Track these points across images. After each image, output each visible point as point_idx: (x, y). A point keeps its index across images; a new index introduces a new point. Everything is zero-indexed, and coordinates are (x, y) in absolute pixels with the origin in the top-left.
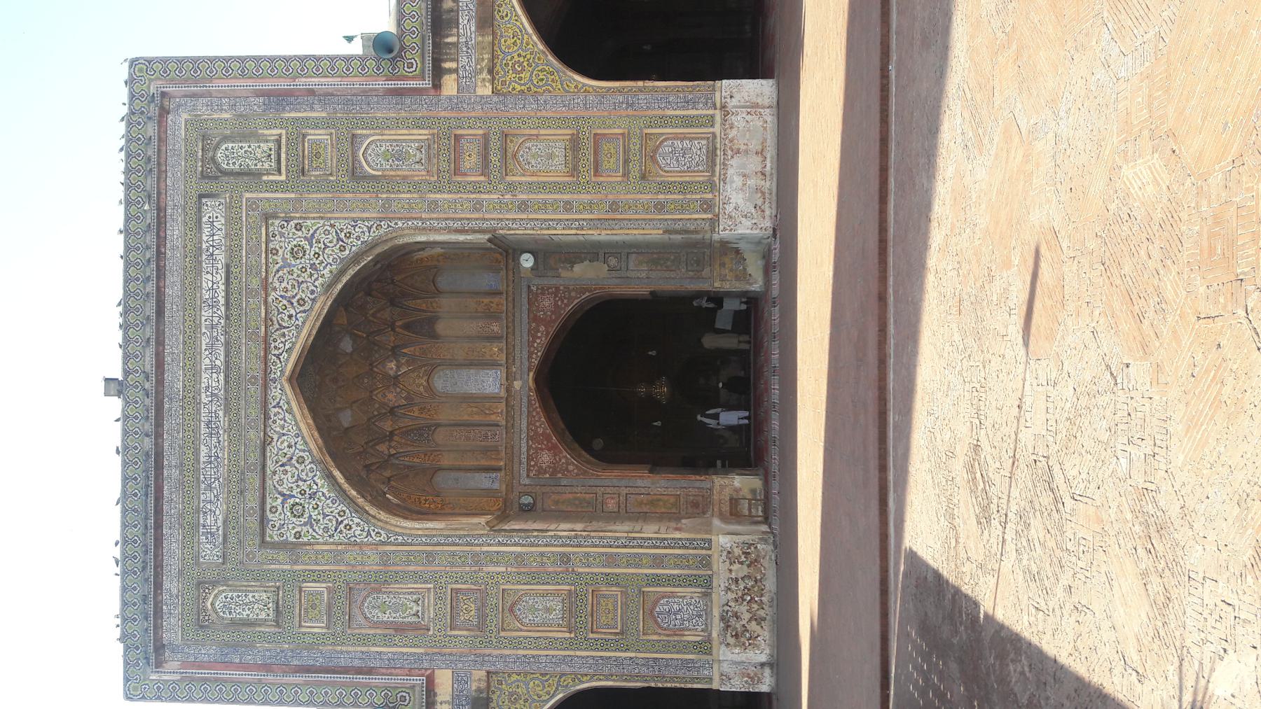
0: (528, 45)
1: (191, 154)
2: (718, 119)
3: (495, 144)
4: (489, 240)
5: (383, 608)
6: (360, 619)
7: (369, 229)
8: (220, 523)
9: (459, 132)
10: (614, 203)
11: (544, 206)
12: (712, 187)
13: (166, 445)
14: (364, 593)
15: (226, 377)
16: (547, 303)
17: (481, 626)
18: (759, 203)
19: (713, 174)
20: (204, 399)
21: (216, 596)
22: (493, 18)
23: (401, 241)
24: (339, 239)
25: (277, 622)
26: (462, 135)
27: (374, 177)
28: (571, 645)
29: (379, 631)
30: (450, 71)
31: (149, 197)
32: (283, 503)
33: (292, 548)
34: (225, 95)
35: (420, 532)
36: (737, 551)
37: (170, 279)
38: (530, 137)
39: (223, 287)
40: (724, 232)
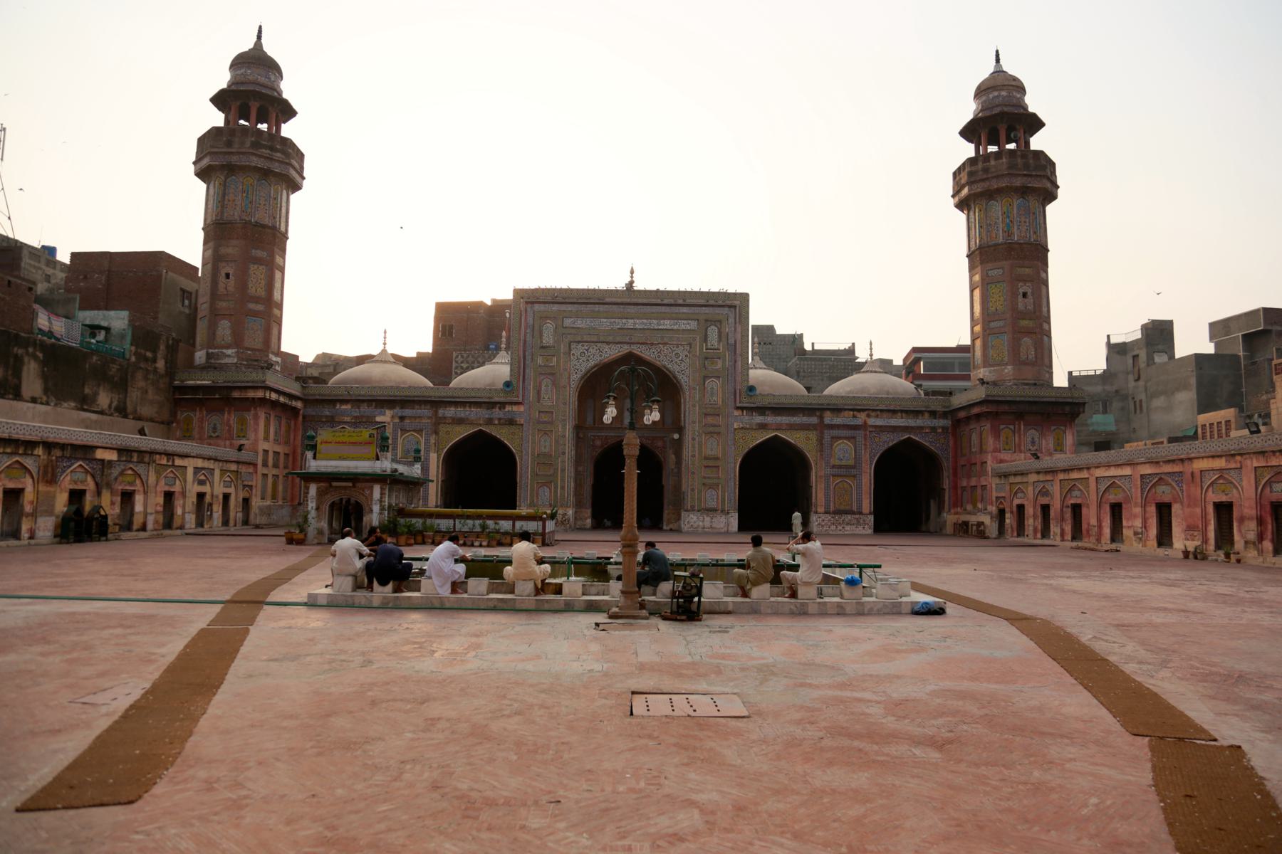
3: (717, 430)
6: (542, 378)
8: (578, 326)
10: (694, 473)
11: (693, 447)
13: (607, 306)
15: (632, 329)
16: (660, 444)
17: (539, 422)
20: (624, 321)
24: (682, 371)
25: (543, 347)
27: (704, 384)
28: (532, 455)
30: (743, 411)
34: (735, 330)
36: (566, 517)
37: (668, 308)
38: (718, 442)
39: (665, 328)
40: (683, 514)
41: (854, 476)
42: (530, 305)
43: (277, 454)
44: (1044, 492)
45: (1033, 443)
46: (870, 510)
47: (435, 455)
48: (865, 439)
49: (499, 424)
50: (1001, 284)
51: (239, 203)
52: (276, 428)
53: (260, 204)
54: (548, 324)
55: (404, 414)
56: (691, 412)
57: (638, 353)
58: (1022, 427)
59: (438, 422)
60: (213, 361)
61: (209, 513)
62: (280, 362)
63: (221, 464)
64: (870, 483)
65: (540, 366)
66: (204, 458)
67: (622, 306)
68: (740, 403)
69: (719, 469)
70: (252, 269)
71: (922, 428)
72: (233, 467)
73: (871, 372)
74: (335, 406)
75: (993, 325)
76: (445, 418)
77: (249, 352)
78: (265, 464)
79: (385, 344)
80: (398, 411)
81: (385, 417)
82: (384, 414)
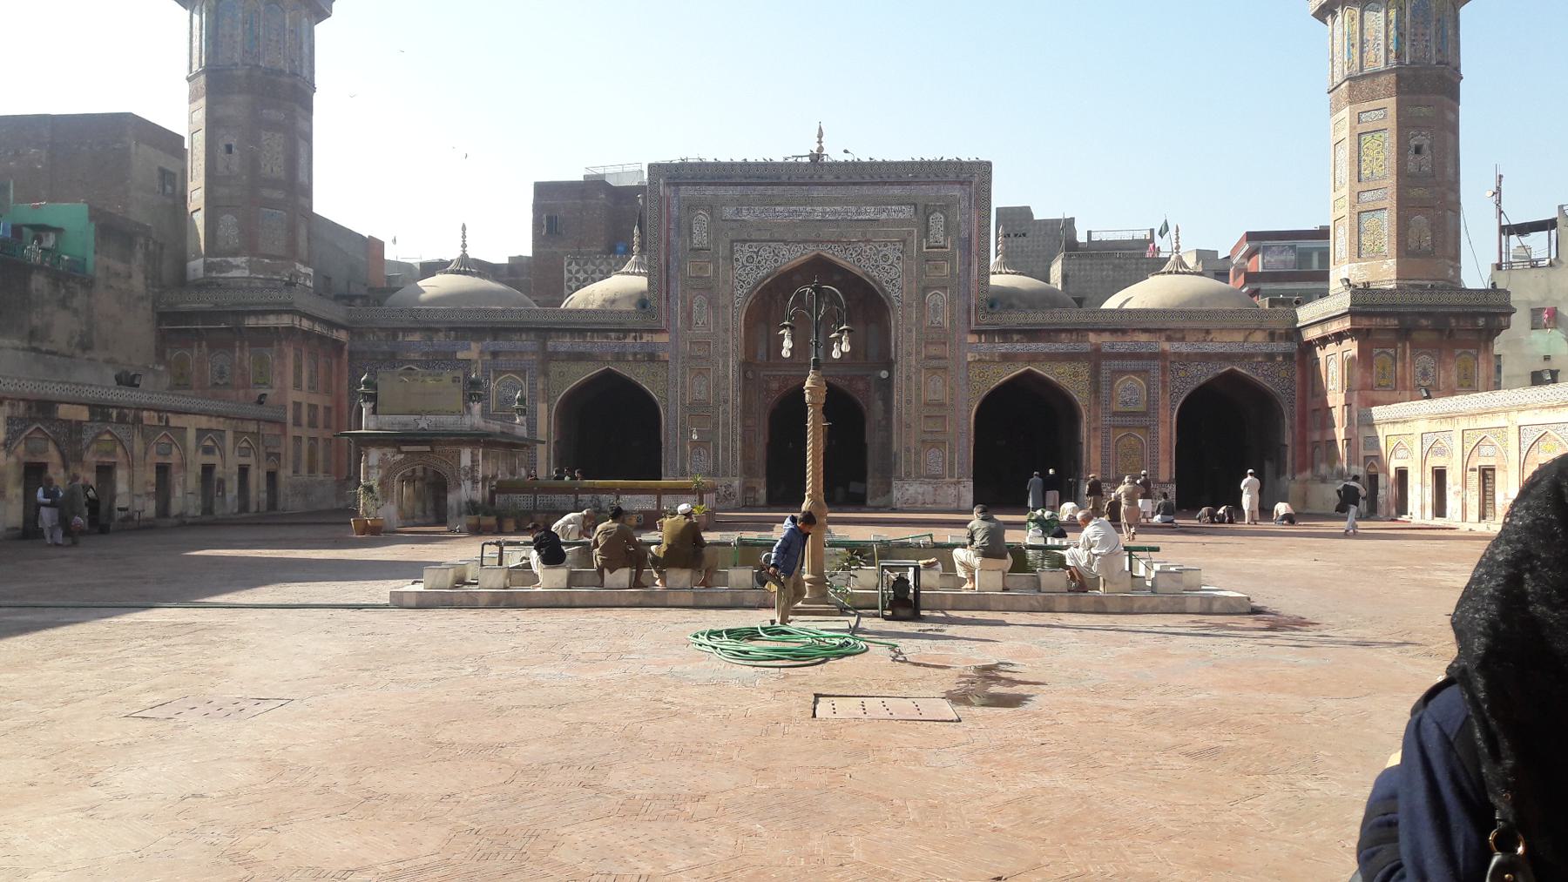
1: (938, 199)
2: (953, 480)
3: (942, 363)
5: (700, 306)
9: (948, 345)
12: (919, 477)
15: (820, 220)
16: (861, 385)
18: (909, 502)
19: (925, 478)
20: (809, 209)
22: (1008, 361)
23: (891, 313)
31: (916, 177)
32: (754, 252)
33: (731, 258)
34: (970, 218)
36: (731, 490)
37: (871, 188)
39: (867, 217)
41: (1147, 428)
42: (673, 188)
43: (313, 408)
44: (1435, 449)
45: (1425, 374)
46: (1171, 477)
47: (545, 406)
48: (1164, 374)
49: (635, 360)
50: (1381, 134)
51: (239, 39)
52: (311, 371)
53: (271, 40)
55: (497, 349)
57: (828, 256)
58: (1408, 351)
59: (550, 357)
60: (214, 274)
61: (220, 494)
62: (312, 274)
63: (235, 422)
64: (1171, 438)
65: (690, 277)
66: (211, 416)
67: (804, 187)
68: (976, 325)
69: (945, 420)
70: (264, 138)
71: (1252, 356)
72: (252, 427)
73: (1177, 272)
74: (395, 336)
75: (1366, 196)
76: (557, 353)
77: (266, 261)
78: (297, 423)
79: (464, 246)
80: (488, 342)
81: (472, 351)
82: (469, 349)
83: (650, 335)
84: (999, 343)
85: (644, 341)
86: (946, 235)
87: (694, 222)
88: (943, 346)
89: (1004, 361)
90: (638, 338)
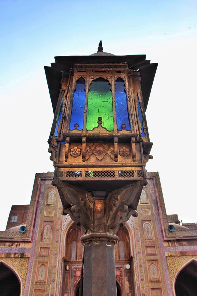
0: (179, 266)
4: (132, 256)
5: (47, 230)
7: (131, 225)
9: (156, 247)
14: (51, 225)
17: (40, 256)
21: (54, 191)
22: (183, 256)
23: (129, 232)
26: (155, 248)
28: (32, 283)
29: (42, 229)
35: (63, 239)
38: (157, 268)
42: (43, 181)
49: (15, 258)
54: (52, 192)
56: (137, 245)
65: (45, 216)
68: (166, 237)
83: (24, 244)
84: (177, 246)
85: (20, 247)
86: (147, 197)
87: (50, 194)
88: (154, 248)
89: (181, 256)
90: (18, 245)
